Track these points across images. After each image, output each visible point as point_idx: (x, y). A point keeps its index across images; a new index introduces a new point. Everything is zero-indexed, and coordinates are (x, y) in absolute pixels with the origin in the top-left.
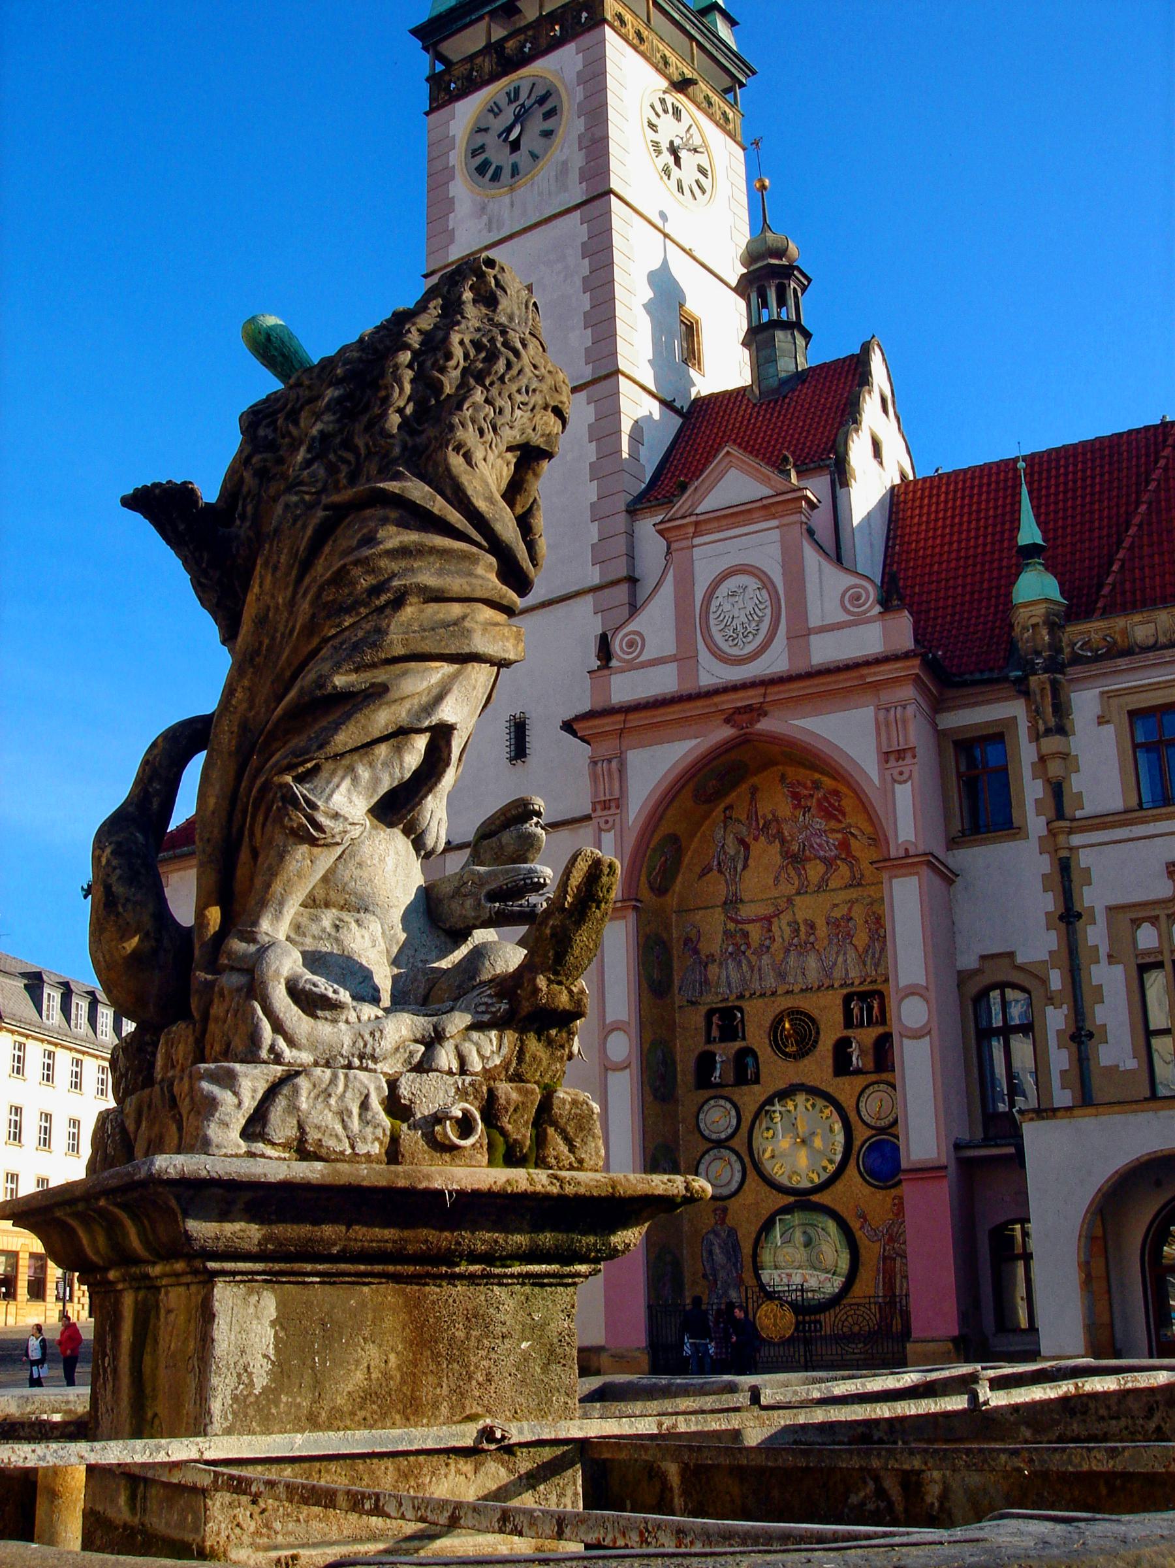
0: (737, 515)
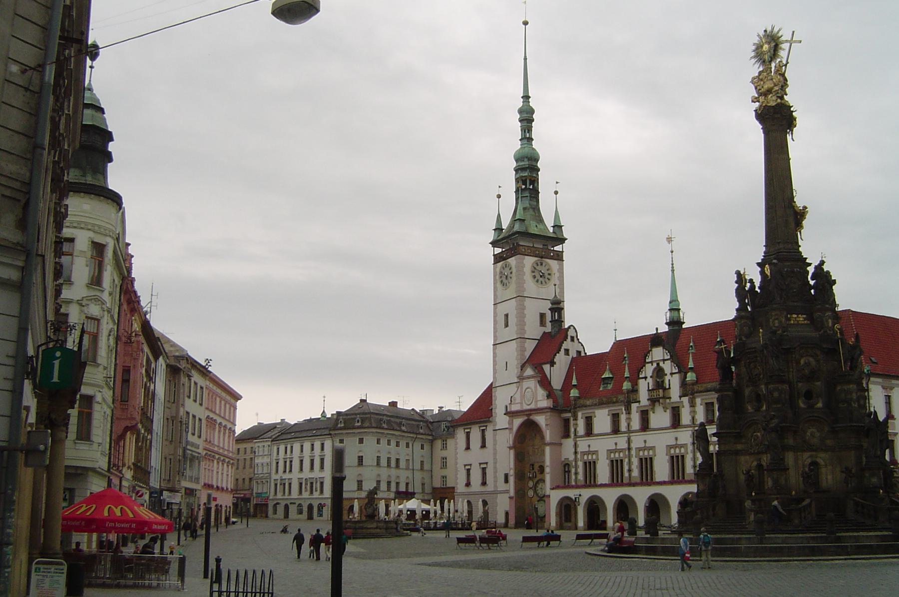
0: (529, 377)
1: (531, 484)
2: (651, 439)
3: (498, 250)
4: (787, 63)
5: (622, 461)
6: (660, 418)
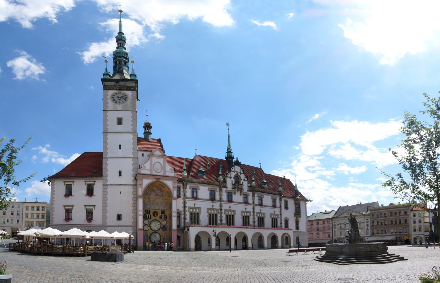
2: (233, 207)
5: (216, 215)
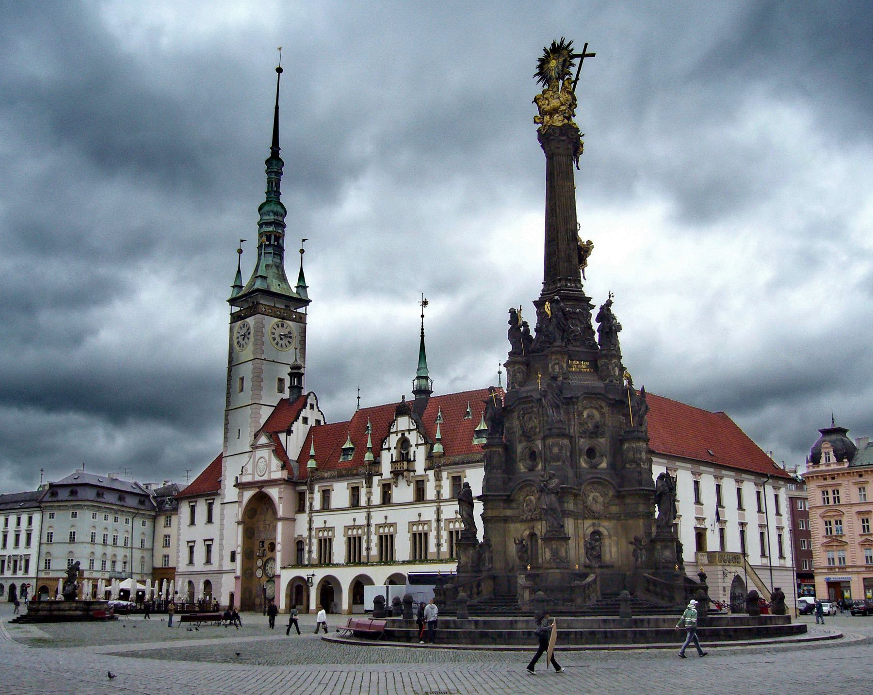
0: (263, 446)
1: (259, 563)
2: (393, 515)
3: (236, 309)
4: (577, 79)
5: (360, 538)
6: (403, 492)
